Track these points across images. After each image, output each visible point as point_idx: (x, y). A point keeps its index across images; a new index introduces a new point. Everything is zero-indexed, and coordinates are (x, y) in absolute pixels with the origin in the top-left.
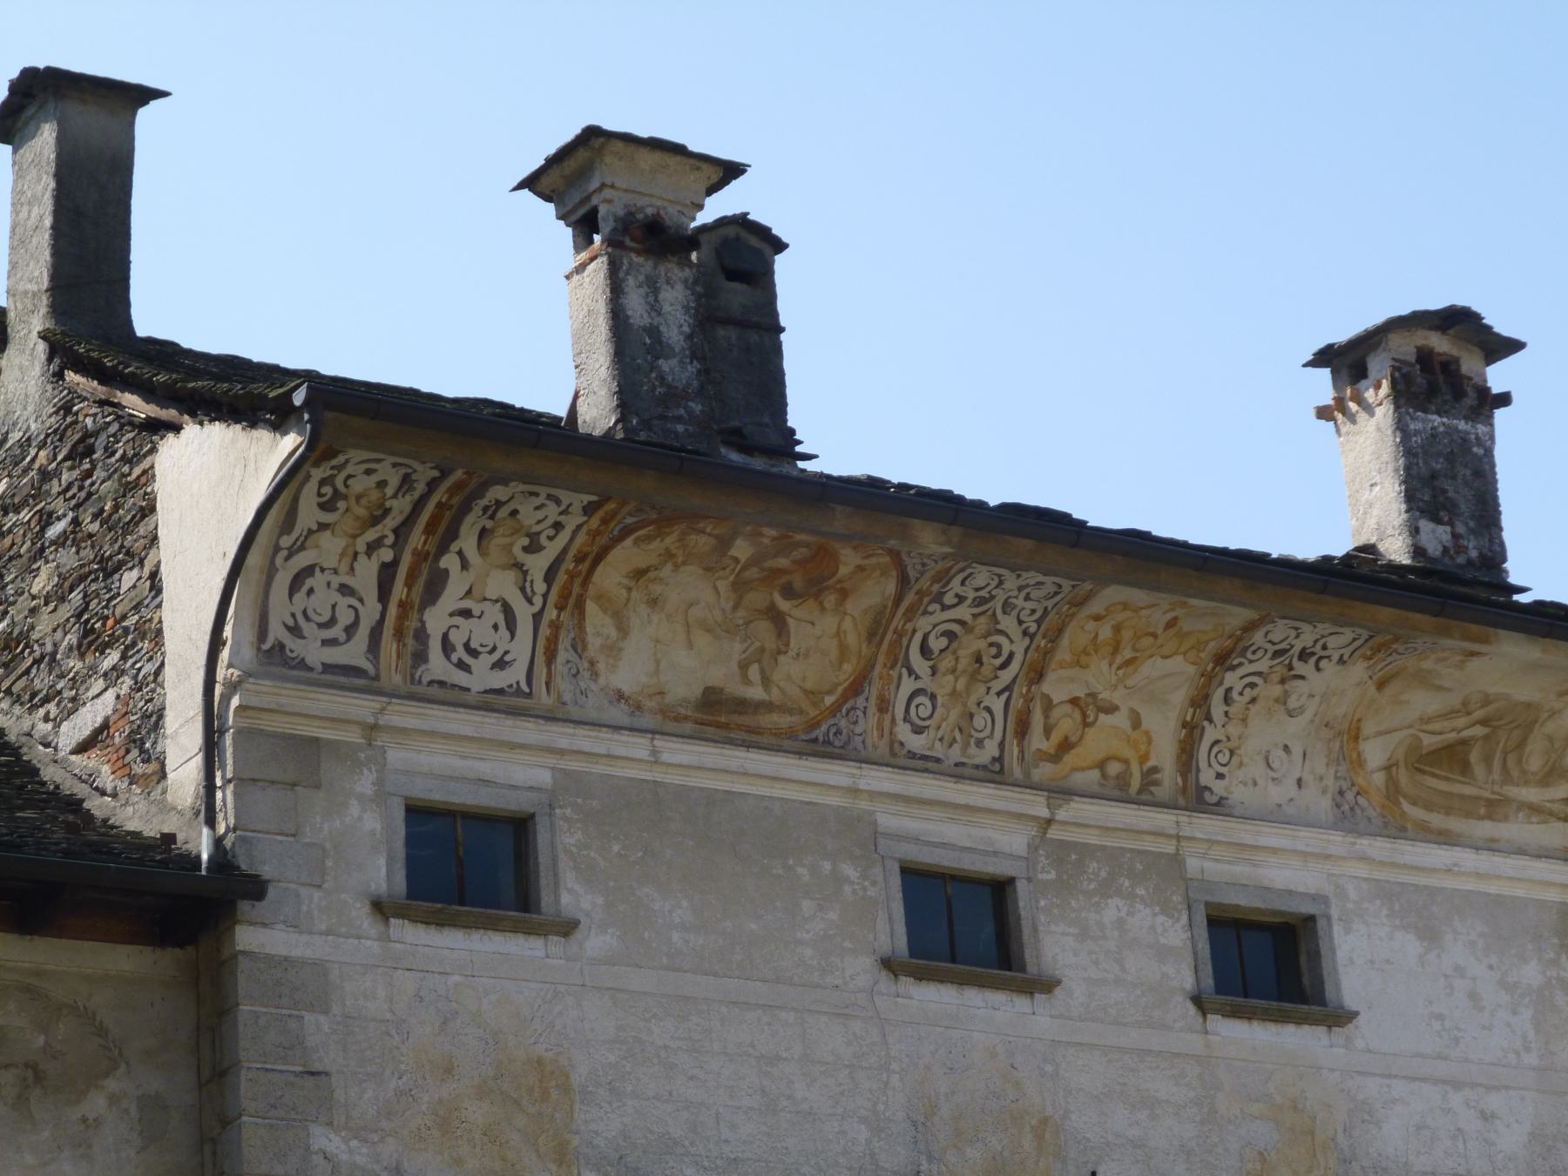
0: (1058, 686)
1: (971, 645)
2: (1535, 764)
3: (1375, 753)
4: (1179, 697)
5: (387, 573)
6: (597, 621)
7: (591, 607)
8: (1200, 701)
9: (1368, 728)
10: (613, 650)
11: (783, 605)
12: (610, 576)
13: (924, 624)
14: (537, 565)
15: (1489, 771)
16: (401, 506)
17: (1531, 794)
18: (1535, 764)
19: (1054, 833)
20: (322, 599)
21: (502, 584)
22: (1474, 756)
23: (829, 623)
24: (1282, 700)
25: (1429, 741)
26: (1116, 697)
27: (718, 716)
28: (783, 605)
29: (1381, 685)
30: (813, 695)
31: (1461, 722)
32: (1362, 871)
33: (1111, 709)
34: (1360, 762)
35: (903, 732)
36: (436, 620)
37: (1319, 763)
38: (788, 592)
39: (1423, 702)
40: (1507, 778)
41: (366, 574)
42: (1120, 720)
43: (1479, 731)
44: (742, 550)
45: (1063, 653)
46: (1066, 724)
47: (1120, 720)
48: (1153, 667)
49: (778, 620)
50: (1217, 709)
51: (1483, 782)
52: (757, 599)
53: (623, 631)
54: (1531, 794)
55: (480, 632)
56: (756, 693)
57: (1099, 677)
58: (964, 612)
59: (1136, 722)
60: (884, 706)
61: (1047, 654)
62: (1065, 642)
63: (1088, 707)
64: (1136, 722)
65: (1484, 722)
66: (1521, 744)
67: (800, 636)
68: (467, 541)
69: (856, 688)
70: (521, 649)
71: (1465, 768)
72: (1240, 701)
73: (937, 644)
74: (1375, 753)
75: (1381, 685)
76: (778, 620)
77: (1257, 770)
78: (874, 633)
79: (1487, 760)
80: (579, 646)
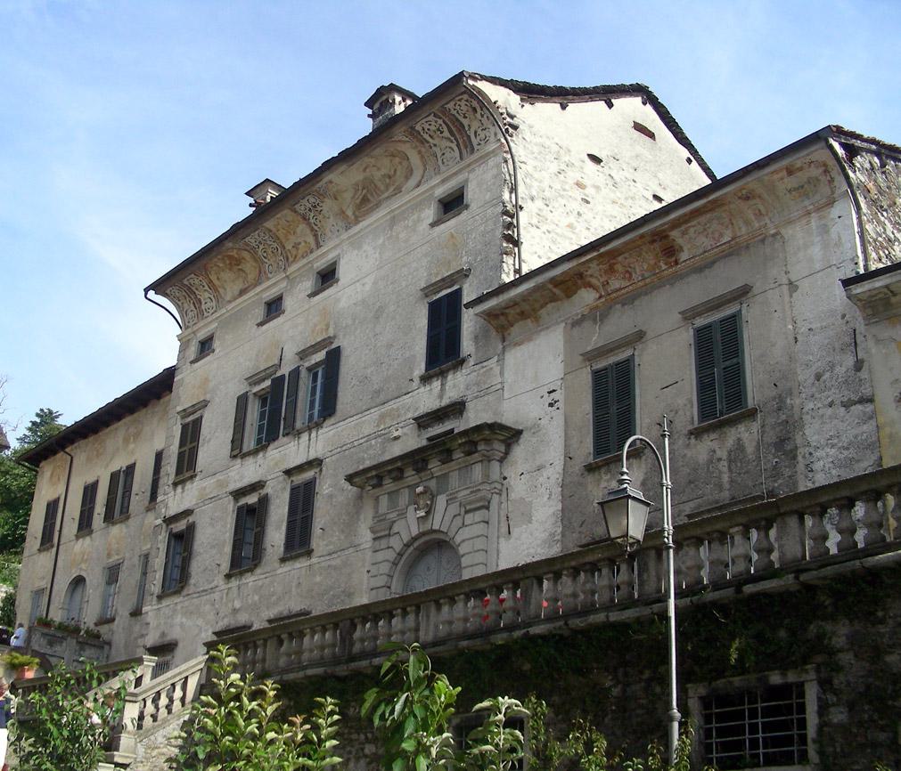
0: (289, 247)
2: (382, 188)
3: (349, 213)
4: (308, 231)
5: (194, 303)
6: (221, 290)
7: (219, 289)
8: (312, 229)
9: (344, 209)
10: (225, 294)
11: (240, 267)
12: (216, 282)
13: (260, 253)
14: (207, 288)
15: (374, 197)
16: (184, 293)
17: (386, 195)
18: (382, 188)
19: (291, 278)
20: (190, 314)
21: (207, 295)
22: (369, 196)
23: (248, 265)
24: (324, 217)
25: (358, 201)
26: (299, 240)
27: (242, 292)
28: (240, 267)
29: (336, 199)
30: (254, 279)
31: (360, 192)
33: (300, 243)
34: (348, 216)
35: (269, 275)
36: (203, 307)
37: (340, 223)
38: (238, 265)
41: (193, 308)
42: (303, 244)
43: (365, 191)
44: (221, 265)
45: (283, 241)
47: (303, 244)
50: (316, 228)
51: (373, 201)
52: (235, 268)
53: (225, 289)
54: (386, 195)
56: (247, 285)
57: (293, 239)
58: (261, 247)
59: (306, 242)
60: (265, 273)
61: (281, 243)
62: (281, 238)
63: (296, 246)
64: (306, 242)
65: (364, 188)
66: (376, 186)
68: (197, 292)
69: (260, 272)
70: (214, 304)
71: (368, 200)
72: (318, 223)
73: (265, 255)
74: (349, 213)
75: (336, 199)
77: (330, 234)
78: (256, 261)
79: (372, 195)
80: (221, 297)
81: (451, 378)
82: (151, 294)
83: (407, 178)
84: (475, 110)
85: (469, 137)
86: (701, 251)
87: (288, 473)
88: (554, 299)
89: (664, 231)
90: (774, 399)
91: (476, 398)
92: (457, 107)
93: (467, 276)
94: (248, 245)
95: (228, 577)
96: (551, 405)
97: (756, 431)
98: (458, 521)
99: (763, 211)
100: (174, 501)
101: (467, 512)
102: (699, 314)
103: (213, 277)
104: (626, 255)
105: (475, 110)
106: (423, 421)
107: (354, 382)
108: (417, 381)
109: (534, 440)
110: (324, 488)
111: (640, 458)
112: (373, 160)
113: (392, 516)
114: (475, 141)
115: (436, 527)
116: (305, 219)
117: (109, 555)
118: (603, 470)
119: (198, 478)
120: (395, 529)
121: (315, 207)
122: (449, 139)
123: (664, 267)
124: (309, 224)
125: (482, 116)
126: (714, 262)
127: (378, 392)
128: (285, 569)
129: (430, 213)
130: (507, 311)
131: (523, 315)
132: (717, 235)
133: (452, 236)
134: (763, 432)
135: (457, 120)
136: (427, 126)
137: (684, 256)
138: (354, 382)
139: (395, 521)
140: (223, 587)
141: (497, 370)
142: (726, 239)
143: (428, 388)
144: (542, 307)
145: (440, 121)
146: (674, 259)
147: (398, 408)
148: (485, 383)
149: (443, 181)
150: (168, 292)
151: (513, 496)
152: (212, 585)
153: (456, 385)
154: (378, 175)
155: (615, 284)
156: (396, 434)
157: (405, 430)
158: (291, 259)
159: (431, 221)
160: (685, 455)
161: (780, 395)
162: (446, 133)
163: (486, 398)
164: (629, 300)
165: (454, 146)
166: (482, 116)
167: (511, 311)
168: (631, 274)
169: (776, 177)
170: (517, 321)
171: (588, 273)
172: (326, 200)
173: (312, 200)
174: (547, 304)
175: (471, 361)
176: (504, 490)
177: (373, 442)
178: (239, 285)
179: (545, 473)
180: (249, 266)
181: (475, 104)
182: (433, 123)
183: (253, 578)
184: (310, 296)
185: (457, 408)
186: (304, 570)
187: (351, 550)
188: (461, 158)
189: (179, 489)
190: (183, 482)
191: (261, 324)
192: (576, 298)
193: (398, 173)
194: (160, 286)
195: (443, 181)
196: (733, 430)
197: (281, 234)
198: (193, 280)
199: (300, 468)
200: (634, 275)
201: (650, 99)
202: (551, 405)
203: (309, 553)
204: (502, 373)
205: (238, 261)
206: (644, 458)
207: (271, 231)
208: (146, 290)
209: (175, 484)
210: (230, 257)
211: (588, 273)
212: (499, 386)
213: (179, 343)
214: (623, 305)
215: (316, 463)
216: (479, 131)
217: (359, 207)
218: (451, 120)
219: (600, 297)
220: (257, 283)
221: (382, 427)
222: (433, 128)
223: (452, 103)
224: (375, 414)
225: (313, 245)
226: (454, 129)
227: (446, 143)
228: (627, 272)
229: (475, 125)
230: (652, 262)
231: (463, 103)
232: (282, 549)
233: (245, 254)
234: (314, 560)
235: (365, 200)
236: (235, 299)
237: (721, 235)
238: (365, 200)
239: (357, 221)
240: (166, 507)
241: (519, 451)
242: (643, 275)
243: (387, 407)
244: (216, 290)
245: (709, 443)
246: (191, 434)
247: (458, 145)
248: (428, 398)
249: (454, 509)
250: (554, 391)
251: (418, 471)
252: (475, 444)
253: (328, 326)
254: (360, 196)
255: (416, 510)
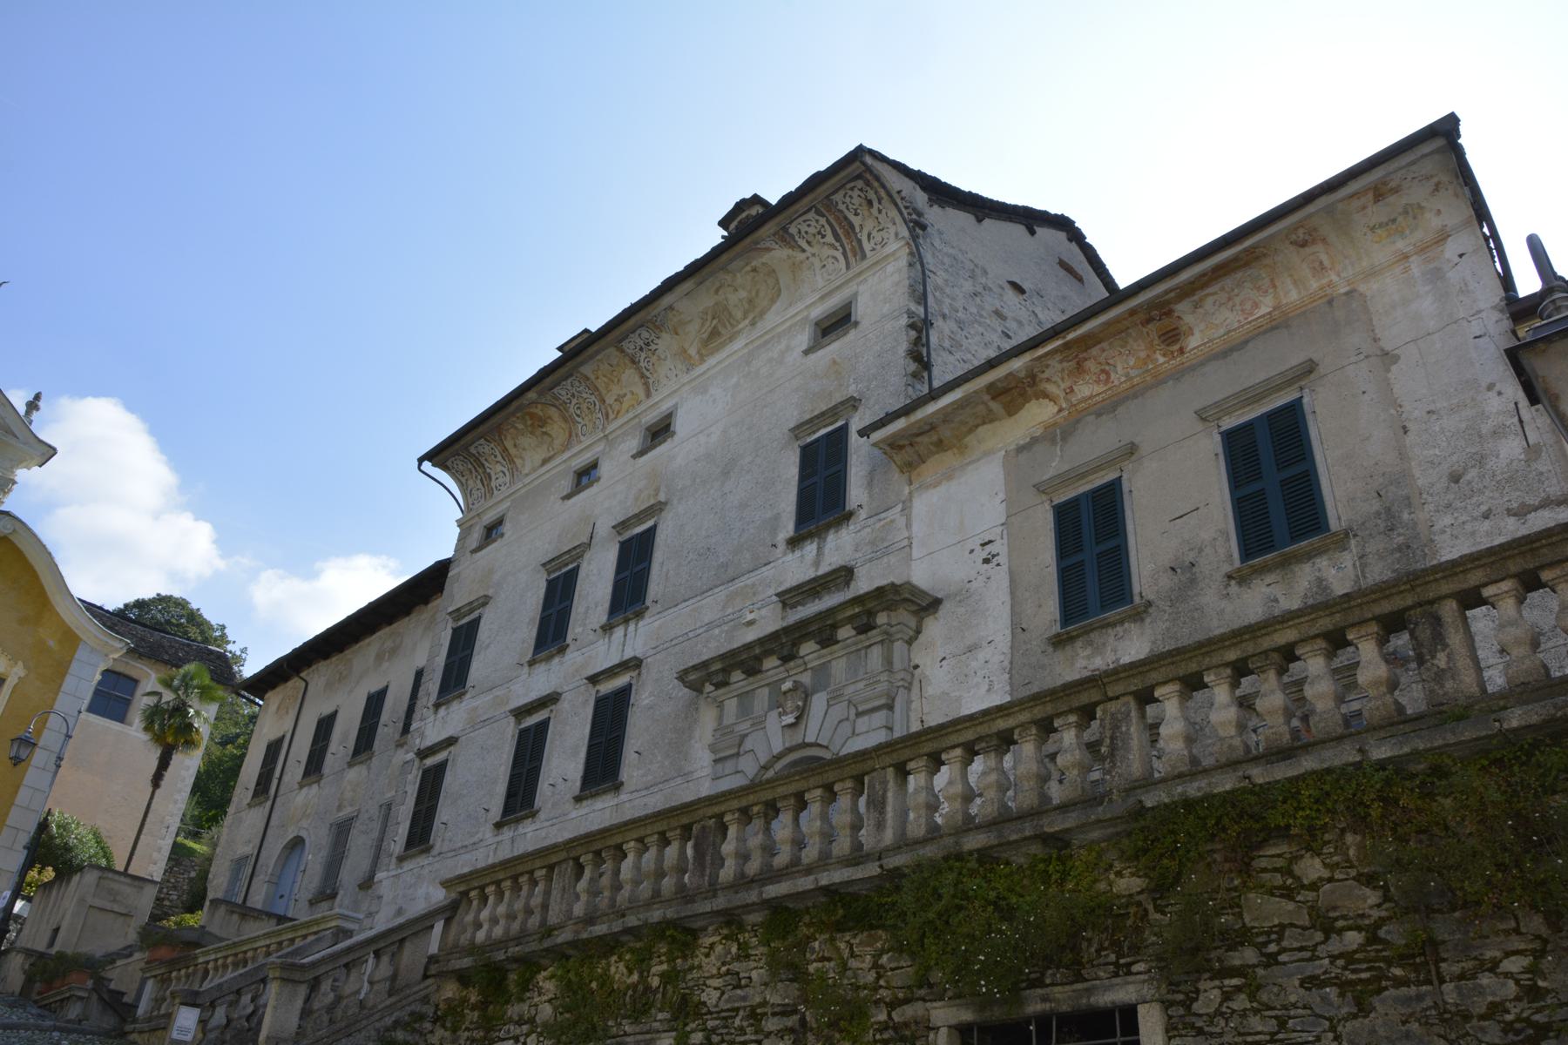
0: (610, 400)
1: (584, 406)
2: (739, 315)
3: (693, 351)
4: (637, 378)
6: (518, 461)
8: (643, 376)
12: (512, 451)
14: (499, 458)
21: (499, 468)
24: (659, 358)
25: (705, 336)
27: (545, 462)
32: (687, 388)
36: (493, 484)
39: (693, 328)
40: (733, 326)
44: (520, 426)
45: (604, 392)
46: (616, 407)
47: (629, 396)
48: (624, 377)
49: (545, 433)
52: (539, 431)
55: (500, 481)
57: (616, 390)
58: (574, 401)
63: (619, 399)
67: (553, 433)
70: (507, 479)
71: (719, 334)
74: (693, 351)
76: (545, 433)
78: (566, 421)
81: (832, 539)
82: (427, 466)
83: (773, 301)
84: (870, 203)
85: (859, 241)
86: (1222, 331)
87: (594, 679)
88: (989, 418)
89: (1169, 302)
90: (1378, 514)
91: (871, 560)
92: (848, 200)
93: (855, 408)
94: (557, 399)
95: (499, 826)
96: (986, 561)
97: (1349, 564)
98: (846, 728)
99: (1326, 263)
100: (431, 728)
101: (859, 715)
102: (1228, 412)
103: (509, 444)
104: (1105, 345)
105: (870, 203)
106: (790, 597)
107: (691, 556)
108: (782, 547)
109: (961, 610)
110: (642, 699)
111: (1142, 620)
112: (728, 277)
113: (744, 727)
114: (867, 246)
115: (810, 739)
116: (633, 362)
117: (340, 808)
118: (1079, 643)
119: (468, 696)
120: (748, 745)
121: (648, 344)
122: (832, 245)
123: (1161, 360)
124: (638, 369)
125: (880, 211)
126: (1246, 342)
127: (725, 566)
128: (583, 811)
129: (803, 339)
130: (919, 439)
131: (940, 446)
132: (1248, 306)
133: (834, 362)
134: (1364, 566)
135: (846, 218)
136: (804, 228)
137: (1193, 342)
138: (691, 556)
139: (746, 735)
140: (490, 841)
141: (901, 522)
142: (1264, 310)
143: (798, 553)
144: (971, 431)
145: (823, 221)
146: (1176, 347)
147: (754, 585)
148: (883, 540)
149: (822, 298)
150: (449, 463)
151: (930, 691)
152: (475, 839)
153: (839, 547)
154: (733, 298)
155: (1084, 390)
156: (750, 617)
157: (764, 612)
158: (612, 416)
159: (804, 347)
160: (1223, 611)
161: (1388, 510)
162: (830, 238)
163: (885, 560)
164: (1108, 408)
165: (839, 254)
166: (880, 211)
167: (925, 439)
168: (1107, 373)
169: (1356, 203)
170: (934, 454)
171: (1045, 375)
172: (664, 335)
173: (645, 334)
174: (977, 426)
175: (863, 514)
176: (916, 684)
177: (717, 631)
178: (538, 458)
179: (982, 655)
180: (557, 429)
181: (871, 195)
182: (813, 223)
183: (533, 827)
184: (634, 457)
185: (845, 574)
186: (608, 812)
187: (679, 780)
188: (848, 267)
189: (442, 711)
190: (448, 702)
191: (568, 497)
192: (1023, 413)
193: (762, 294)
194: (439, 455)
195: (822, 298)
196: (1307, 567)
197: (600, 384)
198: (484, 448)
199: (611, 672)
200: (1113, 376)
201: (1076, 236)
202: (986, 561)
203: (617, 787)
204: (908, 526)
205: (543, 422)
206: (1148, 620)
207: (588, 379)
208: (421, 460)
209: (437, 706)
210: (532, 416)
211: (1045, 375)
212: (906, 542)
213: (458, 530)
214: (1099, 415)
215: (634, 664)
216: (874, 233)
217: (706, 343)
218: (837, 219)
219: (1060, 410)
220: (567, 446)
221: (730, 610)
222: (812, 230)
223: (842, 193)
224: (721, 594)
225: (642, 395)
226: (840, 232)
227: (828, 251)
228: (1103, 371)
229: (869, 225)
230: (1143, 355)
231: (856, 193)
232: (578, 783)
233: (553, 412)
234: (624, 797)
235: (715, 333)
236: (534, 470)
237: (1256, 305)
238: (715, 333)
239: (702, 359)
240: (422, 736)
241: (934, 628)
242: (1127, 375)
243: (739, 584)
244: (512, 461)
245: (1264, 589)
246: (464, 640)
247: (845, 254)
248: (798, 567)
249: (839, 711)
250: (990, 542)
251: (785, 659)
252: (871, 614)
253: (657, 491)
254: (708, 327)
255: (780, 715)
